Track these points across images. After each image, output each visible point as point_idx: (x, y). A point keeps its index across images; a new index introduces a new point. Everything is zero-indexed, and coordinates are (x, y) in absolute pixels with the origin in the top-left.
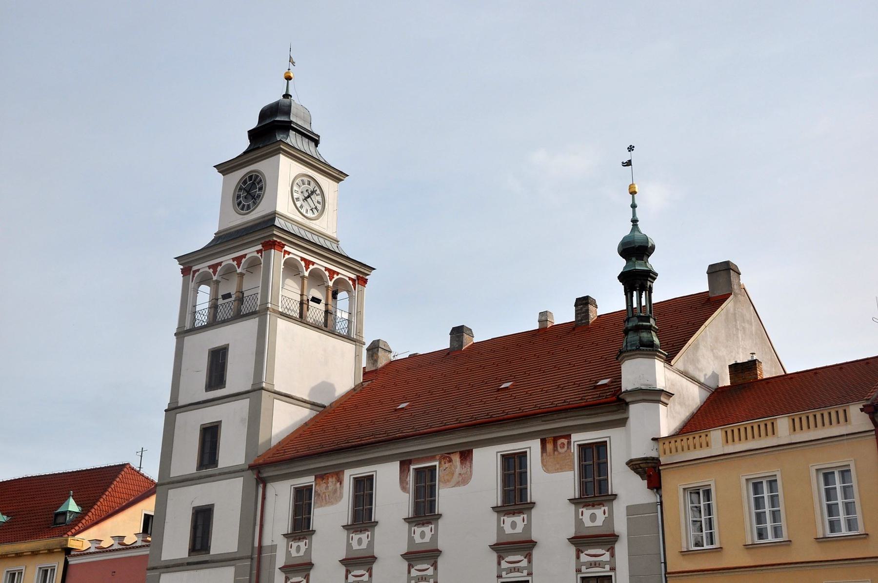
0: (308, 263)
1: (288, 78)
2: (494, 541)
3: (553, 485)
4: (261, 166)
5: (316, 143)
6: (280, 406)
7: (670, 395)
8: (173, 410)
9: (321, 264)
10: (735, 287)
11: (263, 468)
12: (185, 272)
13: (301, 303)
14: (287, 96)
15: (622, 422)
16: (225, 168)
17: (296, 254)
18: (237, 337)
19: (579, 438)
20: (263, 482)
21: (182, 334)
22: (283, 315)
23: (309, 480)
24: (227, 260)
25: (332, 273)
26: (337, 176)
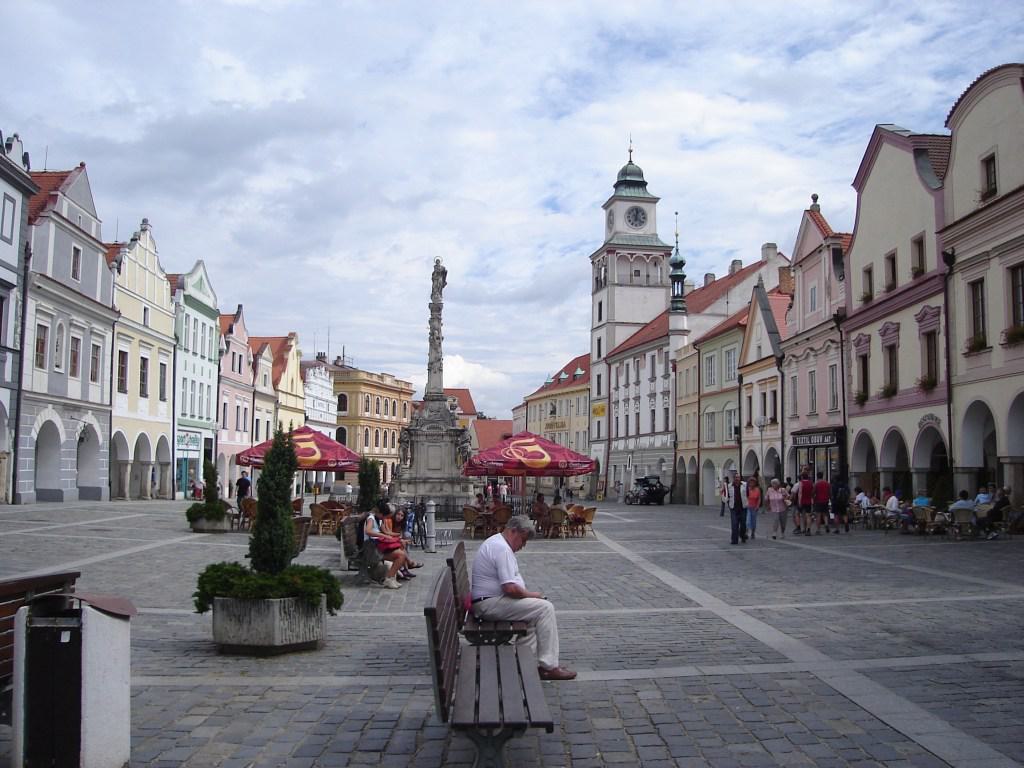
0: (632, 255)
1: (631, 151)
2: (648, 393)
3: (660, 369)
4: (612, 207)
5: (643, 184)
6: (618, 329)
7: (688, 331)
8: (593, 330)
9: (640, 253)
10: (771, 257)
11: (609, 360)
12: (593, 263)
13: (631, 275)
14: (630, 161)
15: (668, 344)
16: (606, 207)
17: (624, 252)
18: (603, 295)
19: (665, 349)
20: (609, 365)
21: (593, 294)
22: (617, 285)
23: (618, 365)
24: (600, 258)
25: (648, 256)
26: (655, 200)
